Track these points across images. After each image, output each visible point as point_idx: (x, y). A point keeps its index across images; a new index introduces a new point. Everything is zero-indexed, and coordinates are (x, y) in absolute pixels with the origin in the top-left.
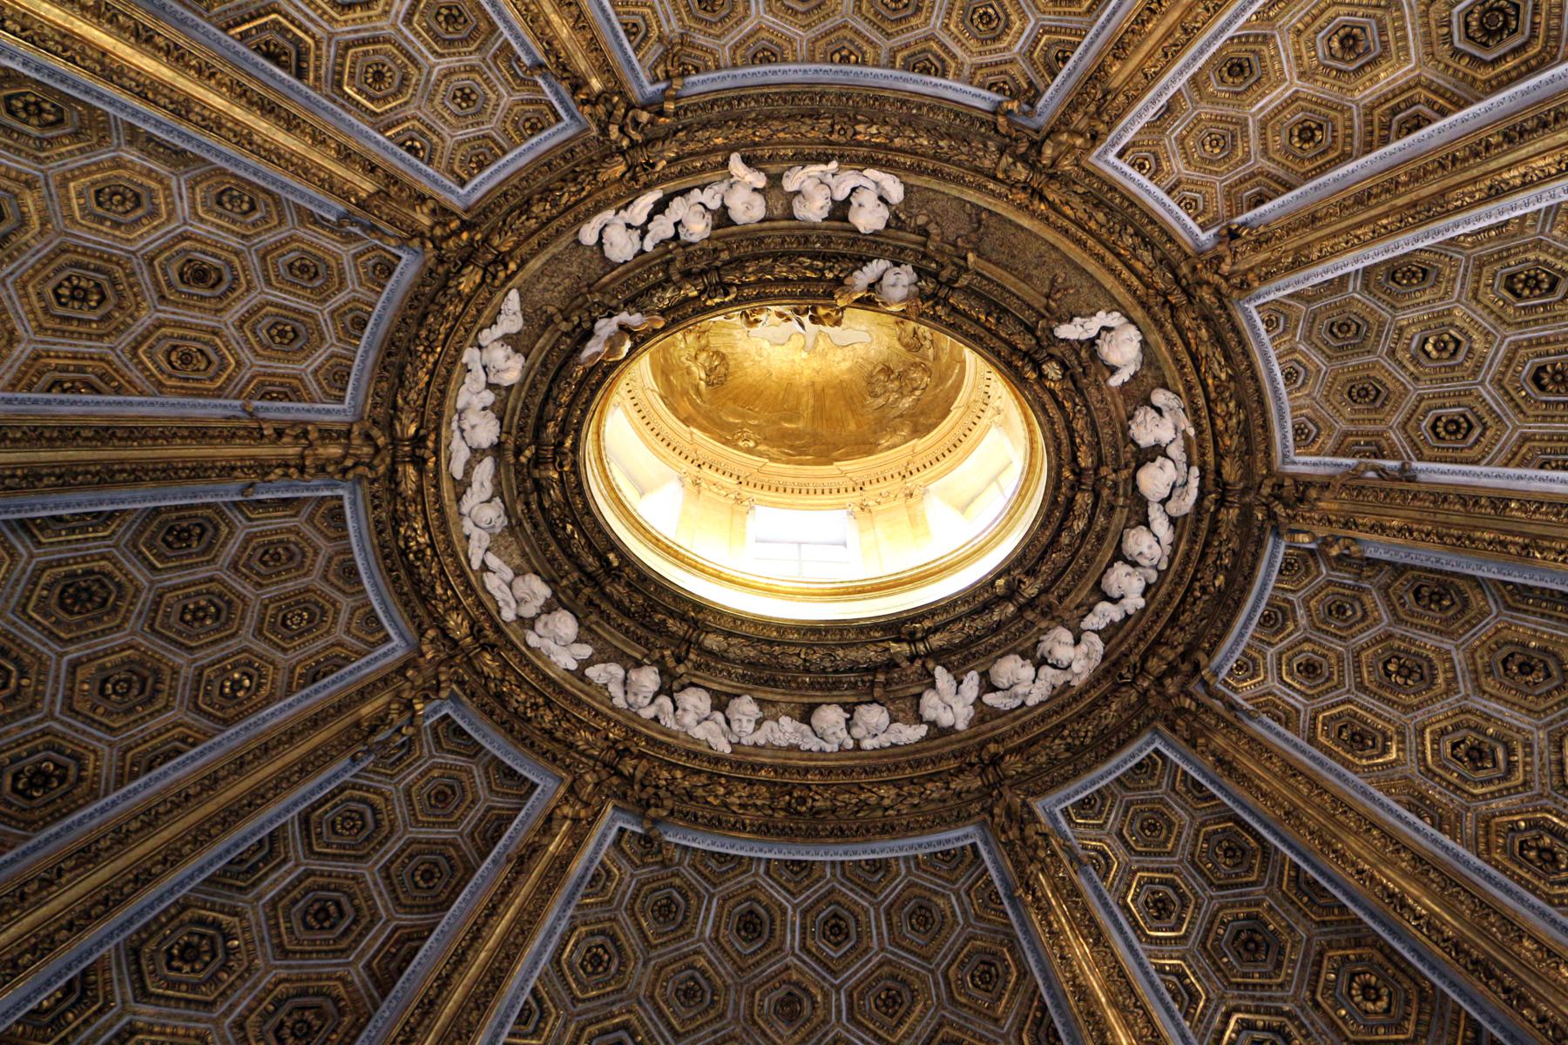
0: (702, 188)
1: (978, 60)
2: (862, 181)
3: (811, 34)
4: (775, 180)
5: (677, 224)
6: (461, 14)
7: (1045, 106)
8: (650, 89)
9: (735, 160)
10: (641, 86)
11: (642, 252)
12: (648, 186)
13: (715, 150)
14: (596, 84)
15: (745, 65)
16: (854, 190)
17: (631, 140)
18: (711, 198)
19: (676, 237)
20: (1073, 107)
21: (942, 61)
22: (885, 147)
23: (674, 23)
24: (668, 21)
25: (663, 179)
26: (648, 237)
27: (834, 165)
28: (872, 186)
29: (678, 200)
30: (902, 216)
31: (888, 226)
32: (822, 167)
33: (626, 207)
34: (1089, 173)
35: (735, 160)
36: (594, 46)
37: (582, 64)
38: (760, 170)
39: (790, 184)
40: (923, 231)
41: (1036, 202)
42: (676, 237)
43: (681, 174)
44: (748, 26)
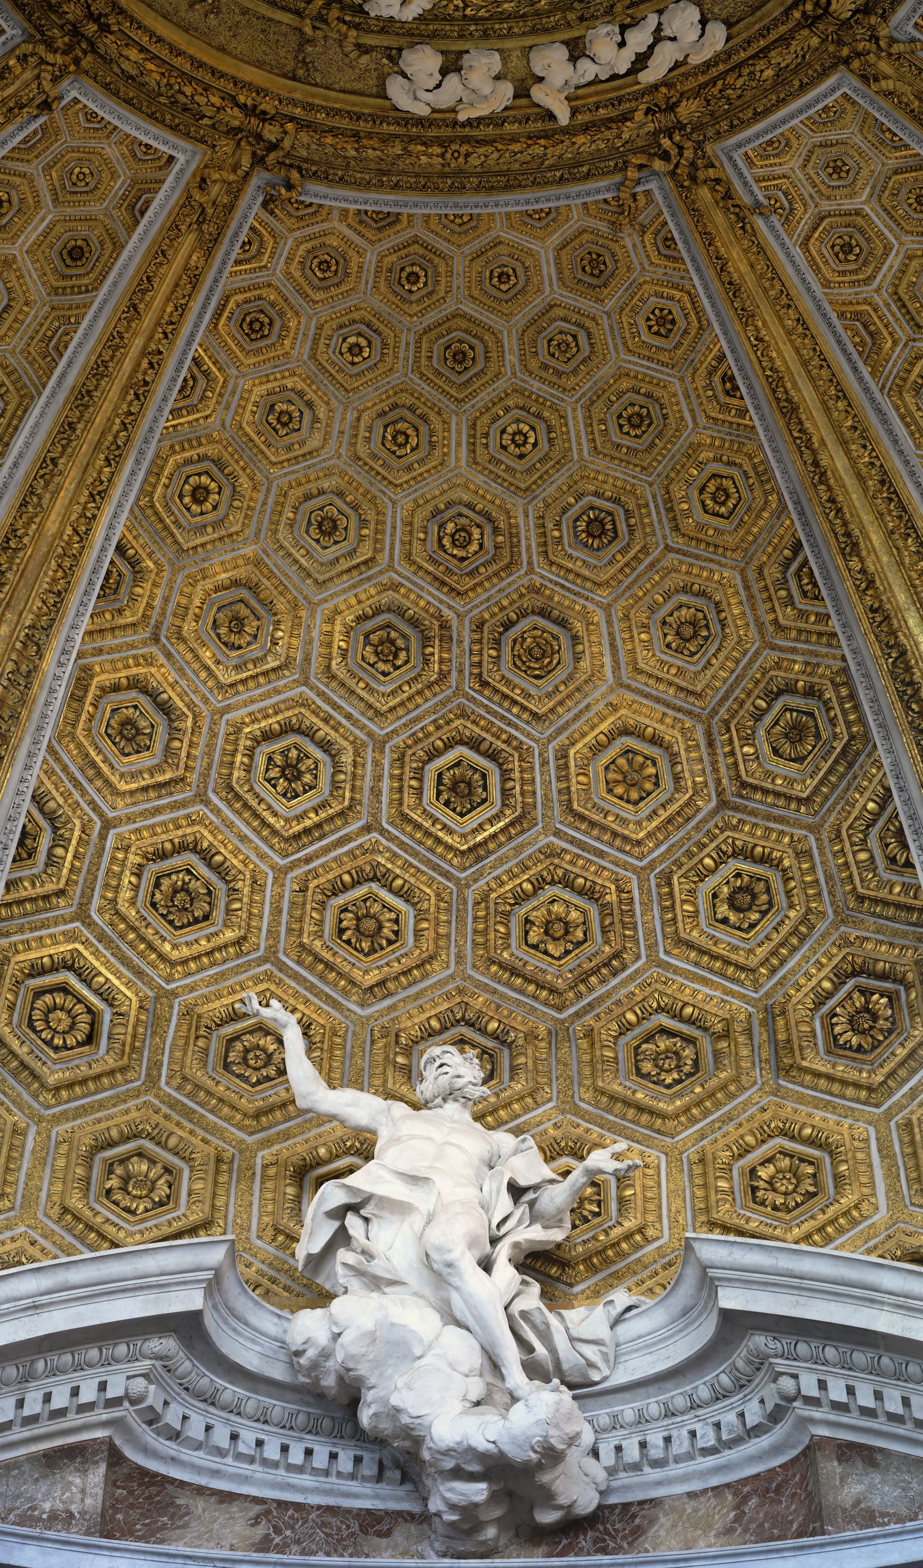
0: (596, 81)
1: (326, 225)
2: (429, 97)
3: (493, 233)
4: (522, 92)
5: (622, 44)
6: (837, 255)
7: (255, 198)
8: (653, 186)
9: (563, 117)
10: (661, 188)
11: (660, 12)
12: (655, 87)
13: (586, 128)
14: (704, 193)
15: (557, 208)
16: (438, 86)
17: (671, 139)
18: (588, 70)
19: (623, 28)
20: (230, 208)
21: (361, 222)
22: (412, 139)
23: (628, 242)
24: (634, 245)
25: (637, 96)
26: (653, 28)
27: (462, 117)
28: (422, 95)
29: (622, 71)
30: (385, 61)
31: (400, 50)
32: (474, 114)
33: (677, 65)
34: (202, 141)
35: (563, 117)
36: (708, 239)
37: (719, 220)
38: (538, 106)
39: (507, 90)
40: (364, 49)
41: (249, 102)
42: (623, 28)
43: (620, 100)
44: (556, 239)
